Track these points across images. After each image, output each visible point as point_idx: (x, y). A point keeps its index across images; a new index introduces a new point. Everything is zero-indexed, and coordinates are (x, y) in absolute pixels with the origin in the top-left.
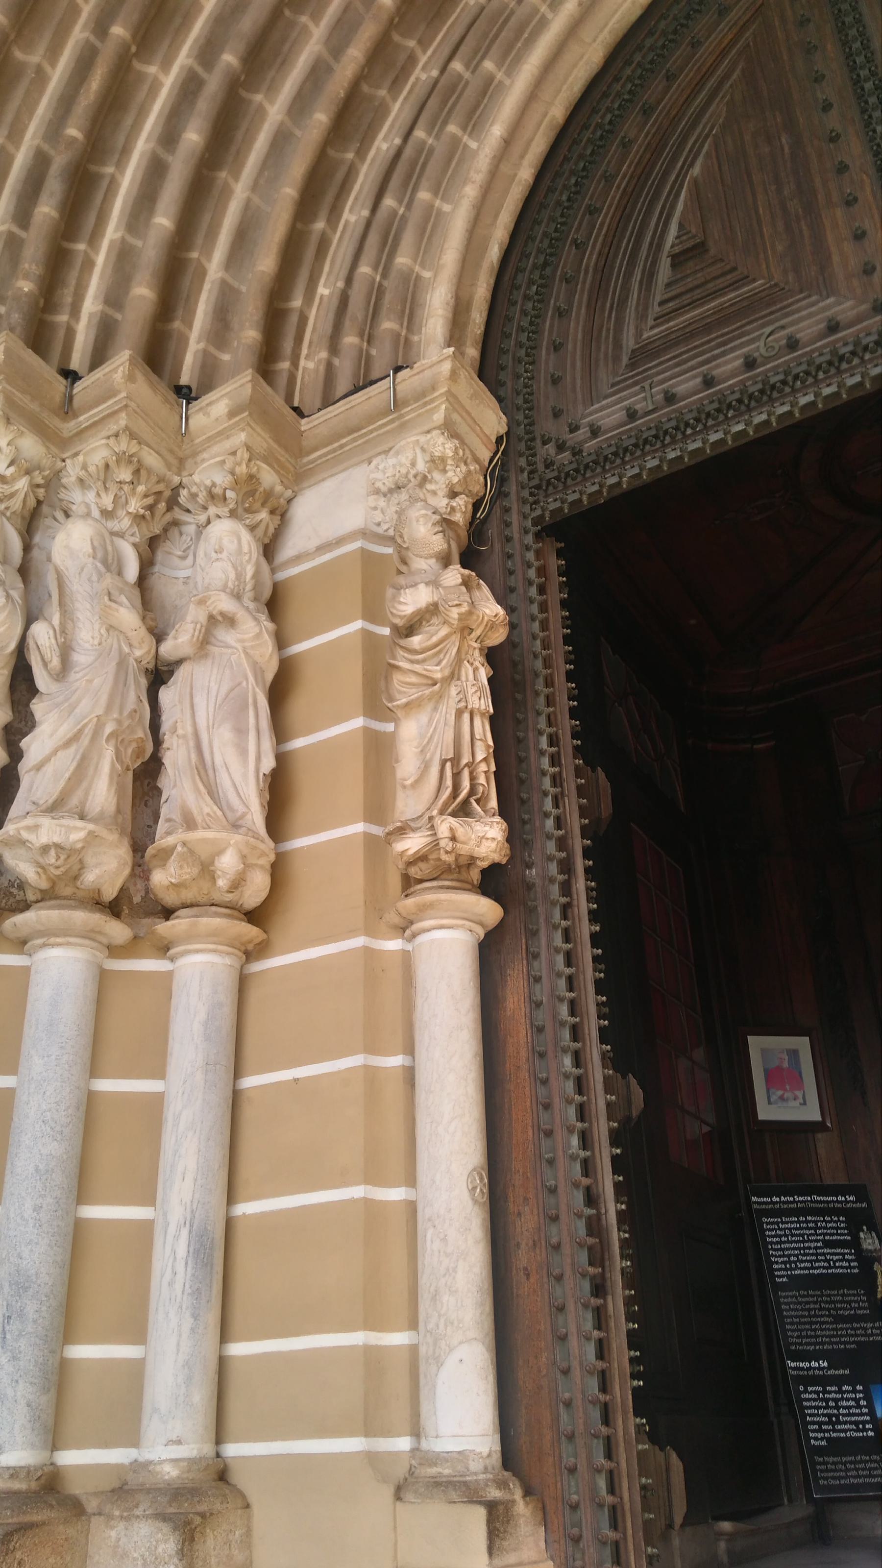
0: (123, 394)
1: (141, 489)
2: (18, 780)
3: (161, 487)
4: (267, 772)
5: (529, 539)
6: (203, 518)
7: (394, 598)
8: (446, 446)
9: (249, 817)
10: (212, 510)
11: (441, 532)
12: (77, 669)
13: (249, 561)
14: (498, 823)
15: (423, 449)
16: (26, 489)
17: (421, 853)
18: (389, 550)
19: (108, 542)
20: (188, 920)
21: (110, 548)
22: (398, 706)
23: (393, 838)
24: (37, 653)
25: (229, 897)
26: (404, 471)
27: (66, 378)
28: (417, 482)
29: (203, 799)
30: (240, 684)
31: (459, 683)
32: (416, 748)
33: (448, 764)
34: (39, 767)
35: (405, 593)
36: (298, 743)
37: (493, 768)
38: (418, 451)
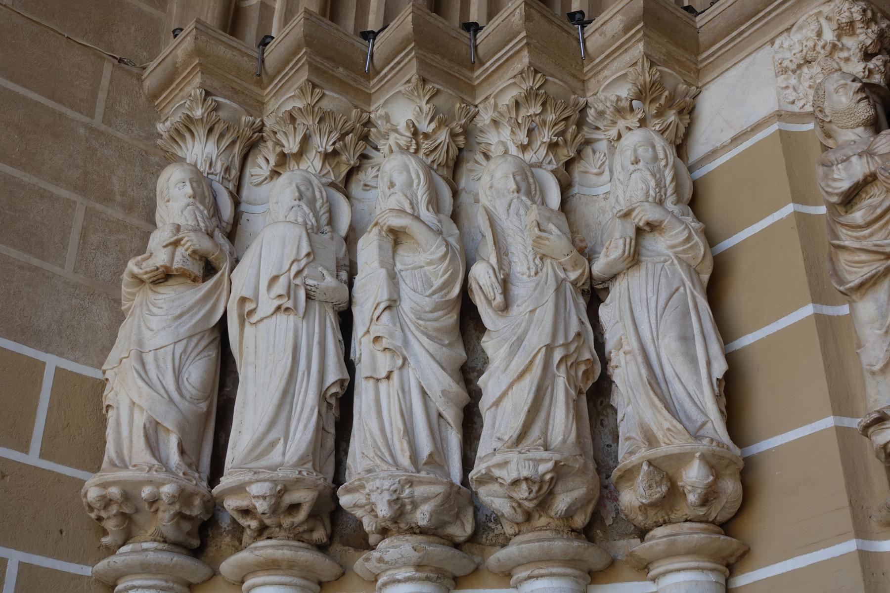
0: (523, 34)
1: (551, 117)
2: (480, 416)
4: (720, 377)
6: (613, 133)
7: (826, 176)
8: (853, 10)
9: (709, 425)
10: (621, 124)
12: (519, 302)
13: (666, 166)
15: (828, 19)
16: (447, 141)
18: (810, 126)
19: (529, 174)
20: (665, 539)
21: (531, 180)
23: (871, 430)
24: (480, 293)
26: (810, 44)
27: (468, 31)
28: (827, 53)
29: (659, 412)
30: (677, 289)
32: (879, 330)
34: (497, 403)
36: (746, 341)
38: (823, 22)
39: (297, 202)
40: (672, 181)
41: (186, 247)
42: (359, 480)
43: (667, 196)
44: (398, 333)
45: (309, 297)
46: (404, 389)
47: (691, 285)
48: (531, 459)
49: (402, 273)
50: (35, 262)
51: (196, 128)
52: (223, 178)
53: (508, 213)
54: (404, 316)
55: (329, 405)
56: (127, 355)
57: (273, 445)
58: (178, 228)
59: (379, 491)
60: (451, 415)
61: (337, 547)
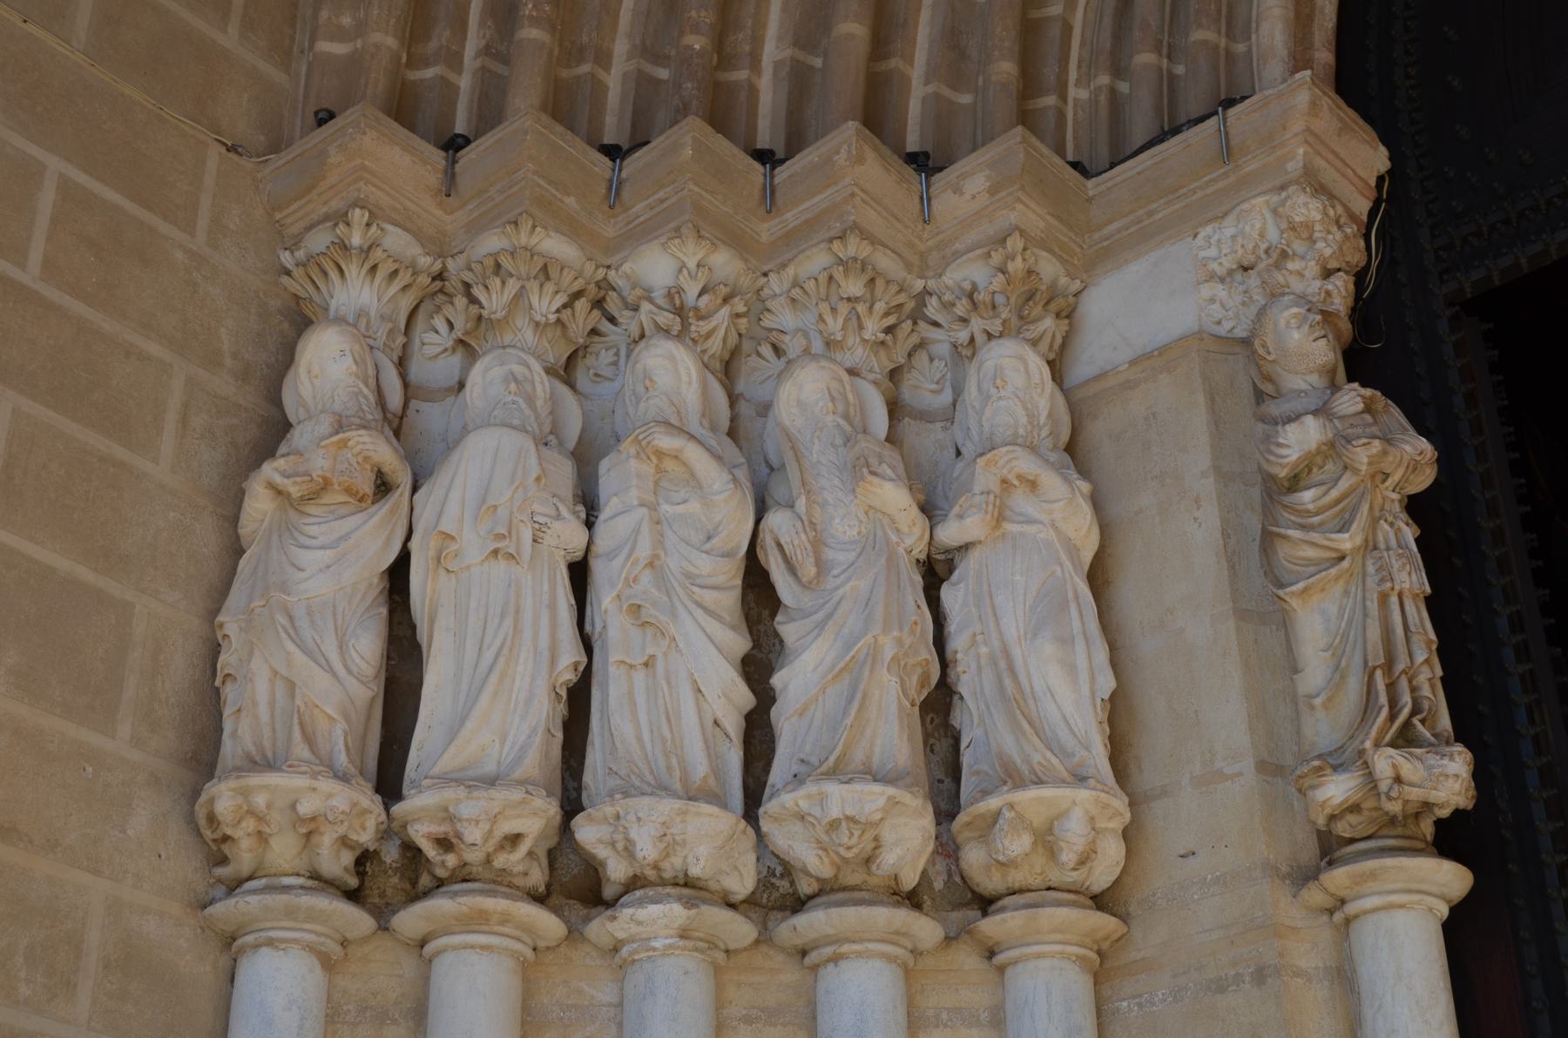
1: (880, 307)
3: (902, 298)
6: (963, 336)
10: (977, 324)
11: (1324, 337)
12: (835, 572)
14: (1460, 753)
16: (726, 323)
17: (1350, 803)
19: (848, 387)
21: (850, 397)
22: (1293, 593)
25: (1072, 877)
33: (1379, 673)
35: (1285, 431)
37: (1439, 672)
41: (355, 451)
43: (1042, 437)
47: (1071, 568)
50: (120, 452)
51: (347, 265)
52: (384, 344)
60: (734, 725)
61: (556, 899)
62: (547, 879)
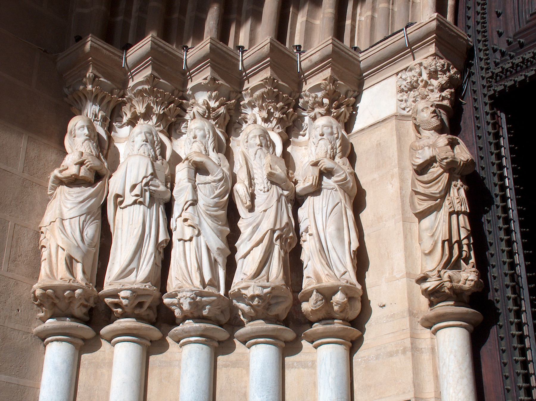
4: (355, 249)
5: (487, 109)
8: (437, 65)
9: (347, 273)
13: (337, 138)
14: (474, 272)
15: (425, 68)
26: (415, 79)
31: (449, 198)
33: (446, 243)
34: (245, 257)
38: (422, 68)
39: (145, 143)
40: (340, 146)
41: (87, 165)
42: (175, 291)
44: (197, 218)
45: (151, 196)
46: (198, 247)
47: (344, 202)
48: (261, 286)
49: (199, 185)
53: (255, 157)
54: (199, 208)
55: (160, 253)
56: (54, 220)
57: (131, 272)
58: (82, 154)
59: (185, 297)
62: (156, 316)
